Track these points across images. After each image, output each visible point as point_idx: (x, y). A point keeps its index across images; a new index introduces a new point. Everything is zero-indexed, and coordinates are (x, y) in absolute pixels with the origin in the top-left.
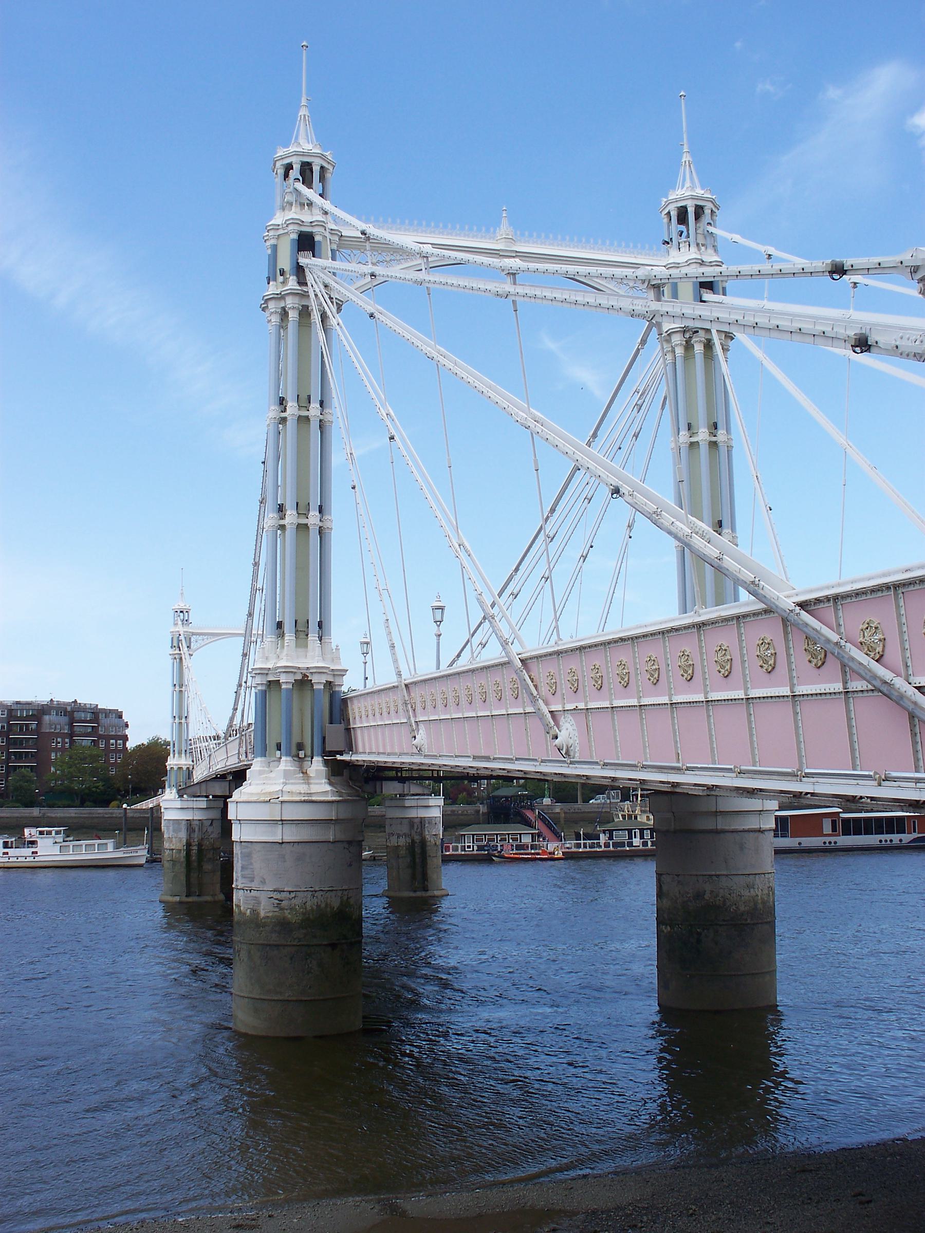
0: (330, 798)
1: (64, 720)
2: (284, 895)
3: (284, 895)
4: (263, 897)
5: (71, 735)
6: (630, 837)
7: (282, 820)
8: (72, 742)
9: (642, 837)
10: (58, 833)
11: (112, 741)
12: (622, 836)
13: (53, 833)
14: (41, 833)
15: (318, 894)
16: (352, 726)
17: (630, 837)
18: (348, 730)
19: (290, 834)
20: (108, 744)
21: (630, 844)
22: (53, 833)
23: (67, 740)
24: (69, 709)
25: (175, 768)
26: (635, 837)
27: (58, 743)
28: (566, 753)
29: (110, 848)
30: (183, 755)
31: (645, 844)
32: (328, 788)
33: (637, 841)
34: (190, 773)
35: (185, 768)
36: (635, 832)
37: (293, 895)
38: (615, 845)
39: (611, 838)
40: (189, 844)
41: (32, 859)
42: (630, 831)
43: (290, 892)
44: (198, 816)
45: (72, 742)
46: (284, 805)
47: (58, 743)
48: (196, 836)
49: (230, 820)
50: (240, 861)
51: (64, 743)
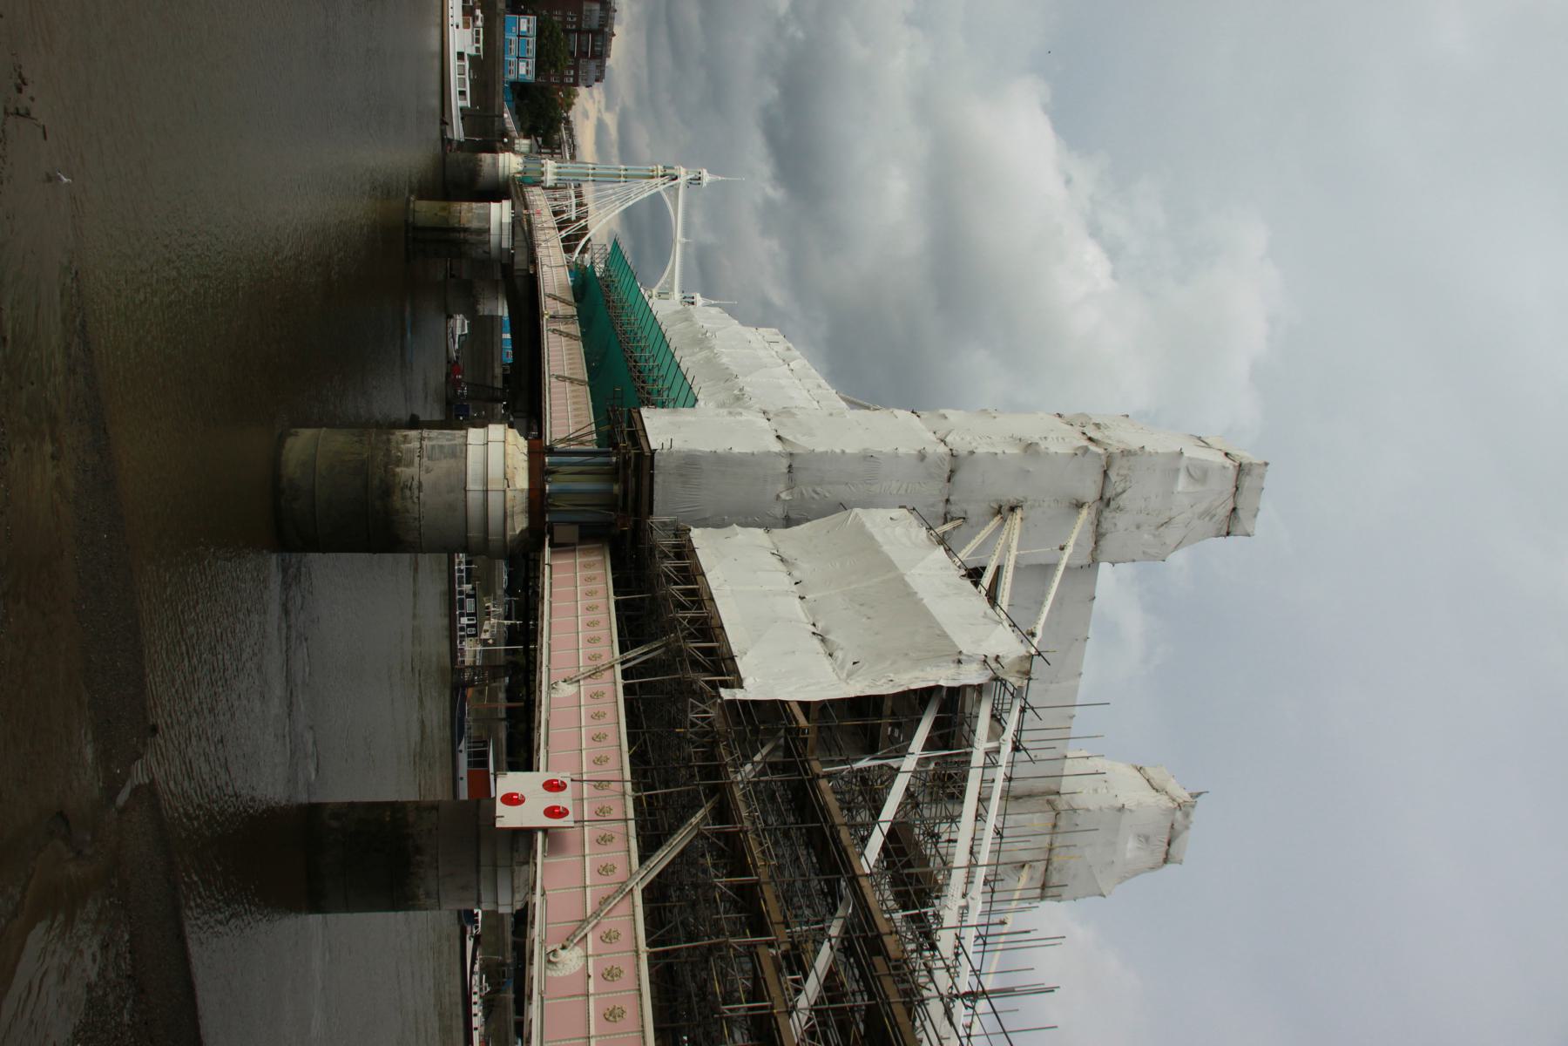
0: (509, 533)
1: (595, 24)
2: (416, 492)
3: (416, 492)
4: (413, 470)
5: (579, 31)
6: (468, 615)
7: (487, 491)
8: (573, 31)
9: (468, 626)
10: (478, 49)
11: (572, 73)
12: (470, 605)
13: (477, 45)
14: (478, 33)
15: (417, 523)
16: (578, 547)
17: (468, 615)
18: (574, 544)
19: (474, 498)
20: (570, 68)
21: (462, 615)
22: (477, 45)
23: (574, 27)
24: (607, 29)
25: (544, 169)
26: (469, 620)
27: (572, 18)
28: (551, 687)
29: (461, 103)
30: (556, 177)
31: (462, 629)
32: (518, 532)
33: (464, 621)
34: (537, 183)
35: (543, 178)
36: (473, 620)
37: (416, 500)
38: (462, 601)
39: (468, 596)
40: (466, 230)
41: (450, 23)
42: (474, 614)
43: (418, 498)
44: (494, 239)
45: (573, 31)
46: (502, 493)
47: (572, 18)
48: (472, 238)
49: (487, 426)
50: (447, 443)
51: (572, 23)
